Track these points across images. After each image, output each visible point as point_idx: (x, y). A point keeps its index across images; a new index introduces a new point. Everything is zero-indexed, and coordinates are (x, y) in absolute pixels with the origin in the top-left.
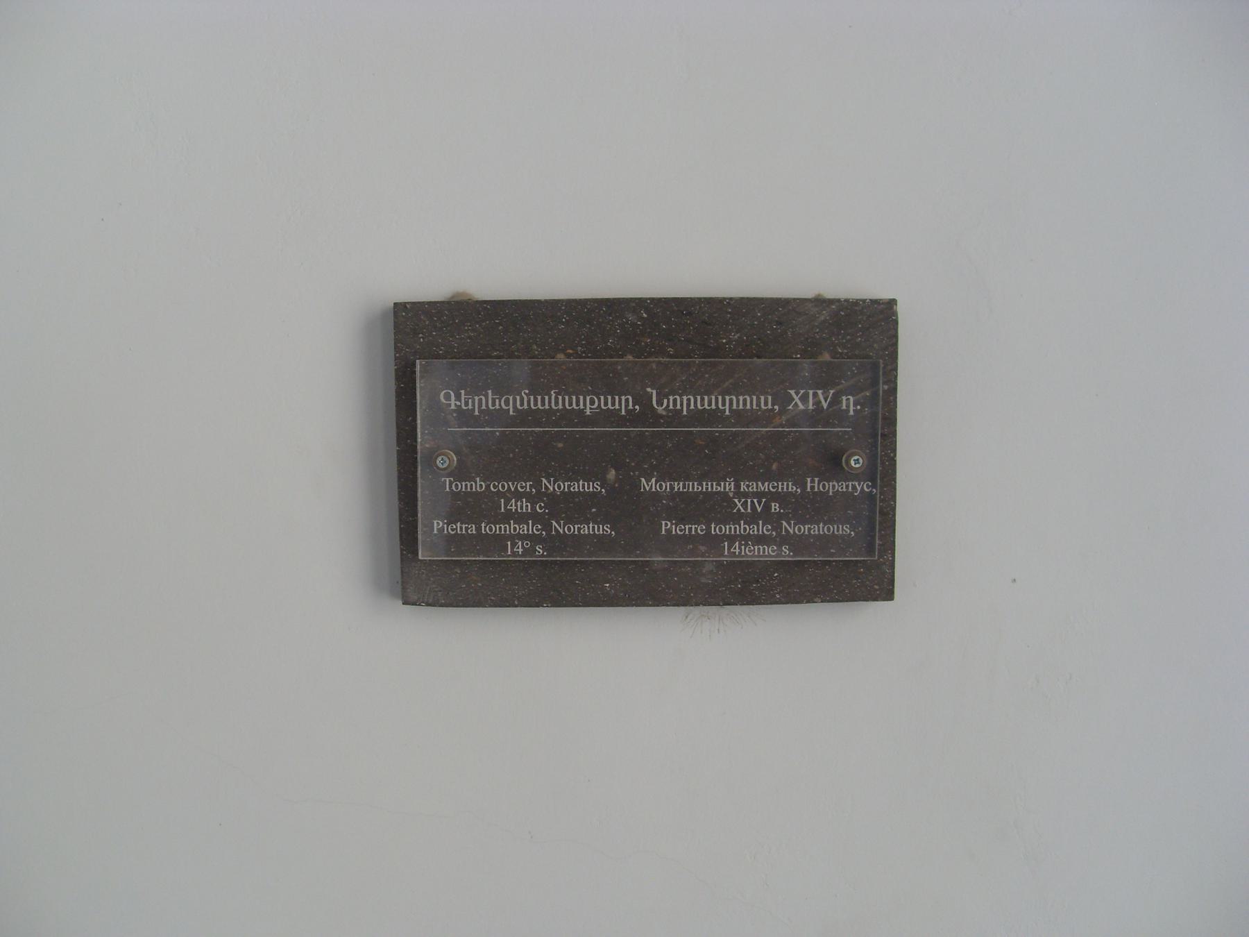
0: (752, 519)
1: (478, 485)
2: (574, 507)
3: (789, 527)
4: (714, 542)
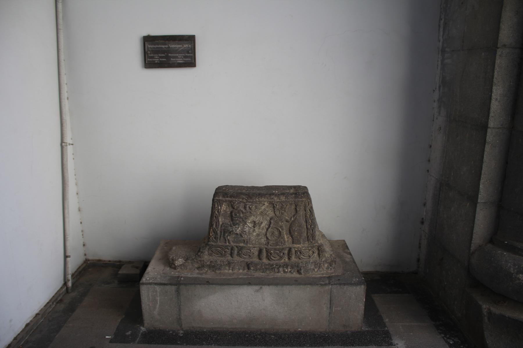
0: (180, 58)
1: (152, 55)
2: (161, 57)
3: (184, 59)
4: (177, 61)
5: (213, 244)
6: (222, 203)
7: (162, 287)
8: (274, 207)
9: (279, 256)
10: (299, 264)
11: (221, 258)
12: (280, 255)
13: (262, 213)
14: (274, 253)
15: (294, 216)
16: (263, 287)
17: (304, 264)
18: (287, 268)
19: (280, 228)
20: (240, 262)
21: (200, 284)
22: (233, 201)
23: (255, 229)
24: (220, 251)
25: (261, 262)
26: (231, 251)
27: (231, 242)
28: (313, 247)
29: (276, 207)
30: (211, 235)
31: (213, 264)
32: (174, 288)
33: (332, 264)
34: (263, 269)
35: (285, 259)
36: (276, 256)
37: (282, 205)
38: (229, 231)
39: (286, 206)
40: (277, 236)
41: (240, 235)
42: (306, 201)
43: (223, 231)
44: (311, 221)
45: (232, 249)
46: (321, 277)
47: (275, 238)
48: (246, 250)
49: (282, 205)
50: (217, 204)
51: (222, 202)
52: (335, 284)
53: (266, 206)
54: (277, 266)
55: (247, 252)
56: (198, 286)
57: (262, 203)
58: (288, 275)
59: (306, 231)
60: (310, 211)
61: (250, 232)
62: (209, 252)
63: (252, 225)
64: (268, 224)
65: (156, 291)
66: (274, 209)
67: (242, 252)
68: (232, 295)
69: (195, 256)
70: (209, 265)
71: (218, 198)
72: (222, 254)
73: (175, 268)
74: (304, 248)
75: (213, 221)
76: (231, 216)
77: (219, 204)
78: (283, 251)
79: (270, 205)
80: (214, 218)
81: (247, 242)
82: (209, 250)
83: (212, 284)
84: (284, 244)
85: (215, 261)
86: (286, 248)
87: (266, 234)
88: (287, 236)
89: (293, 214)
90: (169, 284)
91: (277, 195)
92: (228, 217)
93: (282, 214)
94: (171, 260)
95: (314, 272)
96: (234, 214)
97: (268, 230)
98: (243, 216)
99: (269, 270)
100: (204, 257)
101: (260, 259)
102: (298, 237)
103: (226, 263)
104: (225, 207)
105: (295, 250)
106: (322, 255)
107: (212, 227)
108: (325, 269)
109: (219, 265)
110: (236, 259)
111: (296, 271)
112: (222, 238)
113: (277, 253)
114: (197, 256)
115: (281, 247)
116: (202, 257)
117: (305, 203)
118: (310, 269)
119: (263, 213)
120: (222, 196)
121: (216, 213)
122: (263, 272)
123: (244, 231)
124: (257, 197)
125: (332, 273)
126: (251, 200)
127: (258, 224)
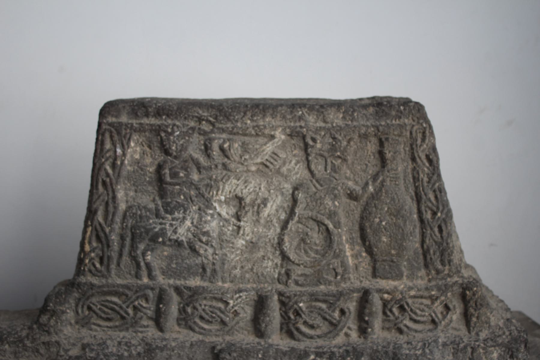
5: (95, 281)
6: (128, 136)
8: (306, 145)
11: (122, 334)
13: (267, 166)
14: (312, 312)
15: (375, 178)
17: (415, 348)
19: (328, 219)
20: (188, 344)
22: (167, 126)
23: (242, 223)
24: (117, 308)
25: (263, 343)
26: (157, 306)
27: (157, 273)
28: (444, 289)
29: (312, 147)
30: (87, 248)
31: (93, 355)
33: (518, 350)
35: (349, 332)
36: (318, 321)
37: (334, 138)
38: (151, 234)
39: (349, 142)
40: (319, 248)
41: (191, 248)
42: (413, 126)
43: (129, 234)
44: (436, 197)
45: (161, 298)
47: (313, 255)
48: (210, 303)
49: (334, 138)
50: (111, 137)
51: (128, 131)
53: (280, 143)
55: (214, 307)
57: (267, 132)
59: (417, 230)
60: (430, 161)
61: (225, 237)
62: (80, 311)
63: (232, 211)
64: (285, 205)
66: (307, 155)
67: (195, 308)
69: (30, 328)
71: (114, 120)
72: (123, 318)
75: (96, 200)
77: (116, 137)
78: (341, 304)
79: (293, 142)
81: (214, 271)
82: (81, 303)
84: (344, 279)
85: (99, 345)
86: (353, 291)
87: (281, 242)
88: (352, 250)
89: (371, 171)
92: (150, 183)
93: (335, 169)
96: (167, 171)
98: (201, 180)
100: (61, 331)
101: (259, 333)
102: (393, 252)
103: (140, 349)
104: (138, 149)
105: (382, 299)
106: (478, 318)
107: (92, 222)
110: (174, 335)
112: (126, 258)
113: (320, 308)
114: (35, 326)
115: (333, 288)
116: (52, 330)
117: (411, 133)
119: (267, 169)
120: (128, 113)
121: (105, 169)
123: (205, 230)
124: (249, 114)
126: (229, 125)
127: (253, 207)
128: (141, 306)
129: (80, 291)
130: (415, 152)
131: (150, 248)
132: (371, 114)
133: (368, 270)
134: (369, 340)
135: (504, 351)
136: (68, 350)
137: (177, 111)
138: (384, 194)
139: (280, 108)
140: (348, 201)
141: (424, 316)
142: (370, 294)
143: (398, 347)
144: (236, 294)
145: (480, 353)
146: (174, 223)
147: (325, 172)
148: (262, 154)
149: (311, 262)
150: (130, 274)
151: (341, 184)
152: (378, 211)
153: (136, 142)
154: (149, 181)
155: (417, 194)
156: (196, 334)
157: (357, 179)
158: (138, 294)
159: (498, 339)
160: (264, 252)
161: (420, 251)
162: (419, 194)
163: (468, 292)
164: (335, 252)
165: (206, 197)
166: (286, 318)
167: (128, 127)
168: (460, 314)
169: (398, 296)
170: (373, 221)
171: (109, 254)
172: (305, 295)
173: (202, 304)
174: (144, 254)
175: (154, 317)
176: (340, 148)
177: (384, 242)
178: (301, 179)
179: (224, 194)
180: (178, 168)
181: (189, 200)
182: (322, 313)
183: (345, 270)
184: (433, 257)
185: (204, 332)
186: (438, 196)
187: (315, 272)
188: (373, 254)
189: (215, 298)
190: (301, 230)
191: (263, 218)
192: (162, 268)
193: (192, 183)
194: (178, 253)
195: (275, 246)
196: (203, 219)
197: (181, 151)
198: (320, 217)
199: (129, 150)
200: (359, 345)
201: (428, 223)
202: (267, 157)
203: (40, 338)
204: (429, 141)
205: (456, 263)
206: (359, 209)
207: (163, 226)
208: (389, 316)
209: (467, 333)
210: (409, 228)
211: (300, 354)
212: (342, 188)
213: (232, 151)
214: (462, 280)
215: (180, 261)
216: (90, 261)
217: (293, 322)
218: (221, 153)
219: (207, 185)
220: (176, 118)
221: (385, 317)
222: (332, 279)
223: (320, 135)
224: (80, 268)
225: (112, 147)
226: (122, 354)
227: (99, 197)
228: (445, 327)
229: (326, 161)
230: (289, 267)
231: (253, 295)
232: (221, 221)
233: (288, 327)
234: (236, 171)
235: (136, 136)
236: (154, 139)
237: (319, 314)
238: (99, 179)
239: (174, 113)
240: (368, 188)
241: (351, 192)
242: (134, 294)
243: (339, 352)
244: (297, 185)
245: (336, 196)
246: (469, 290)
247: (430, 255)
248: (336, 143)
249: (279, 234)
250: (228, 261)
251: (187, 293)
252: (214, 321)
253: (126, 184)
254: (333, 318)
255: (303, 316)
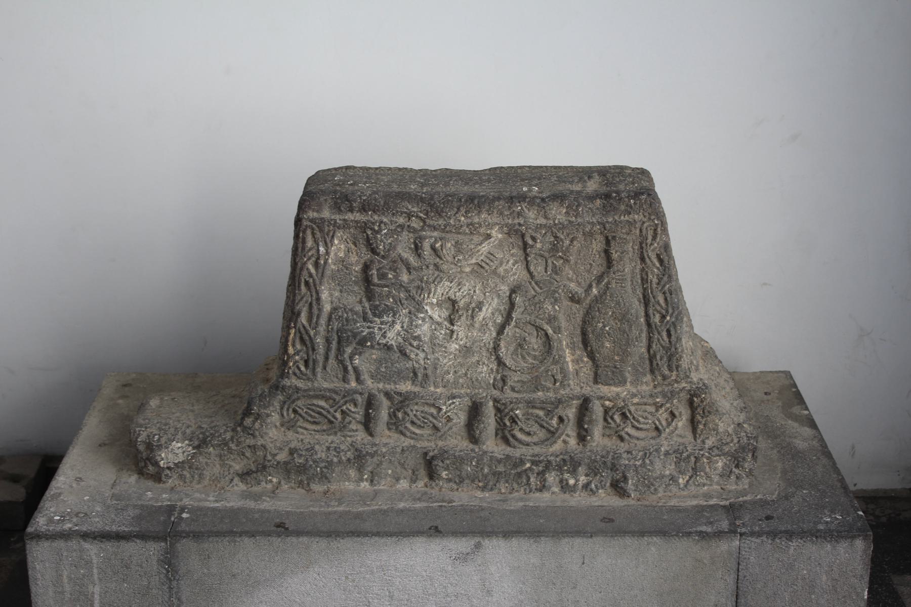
5: (300, 384)
6: (331, 234)
7: (109, 546)
8: (525, 246)
9: (544, 430)
10: (617, 457)
11: (330, 438)
12: (548, 424)
13: (482, 267)
14: (528, 419)
15: (599, 279)
16: (486, 542)
17: (635, 459)
18: (574, 472)
19: (547, 324)
20: (399, 450)
21: (252, 535)
22: (373, 224)
23: (455, 328)
24: (325, 413)
25: (477, 450)
26: (367, 410)
27: (365, 376)
29: (532, 247)
30: (291, 350)
32: (154, 549)
33: (744, 459)
34: (485, 476)
35: (568, 439)
36: (535, 428)
37: (556, 237)
39: (572, 241)
40: (537, 353)
41: (400, 351)
42: (644, 223)
43: (336, 338)
44: (666, 299)
45: (370, 403)
46: (700, 509)
47: (531, 361)
48: (421, 408)
49: (556, 237)
50: (313, 234)
52: (752, 534)
54: (537, 465)
56: (246, 540)
58: (579, 499)
59: (644, 335)
60: (661, 261)
62: (285, 414)
63: (445, 314)
64: (502, 308)
65: (89, 563)
66: (527, 255)
67: (405, 413)
68: (372, 573)
69: (234, 430)
70: (286, 463)
71: (315, 215)
72: (331, 422)
73: (158, 477)
74: (636, 400)
75: (299, 301)
76: (367, 281)
77: (318, 235)
78: (560, 411)
80: (303, 287)
82: (286, 406)
83: (299, 533)
84: (563, 385)
85: (307, 450)
86: (572, 399)
87: (496, 348)
90: (134, 536)
91: (538, 201)
92: (356, 283)
93: (556, 270)
94: (141, 448)
95: (674, 489)
96: (374, 272)
97: (503, 333)
99: (507, 482)
101: (474, 439)
102: (616, 358)
103: (349, 454)
104: (342, 246)
105: (603, 406)
106: (705, 425)
108: (716, 478)
109: (323, 465)
110: (385, 440)
111: (608, 484)
112: (332, 361)
114: (239, 429)
115: (551, 394)
116: (257, 433)
117: (641, 231)
118: (662, 476)
119: (482, 270)
120: (330, 207)
121: (308, 269)
122: (483, 489)
123: (416, 334)
124: (463, 210)
125: (744, 493)
126: (441, 222)
127: (467, 311)
128: (350, 410)
129: (284, 394)
130: (644, 251)
131: (358, 351)
132: (598, 209)
133: (589, 375)
134: (588, 447)
135: (730, 461)
136: (276, 455)
137: (384, 206)
138: (608, 297)
139: (497, 203)
140: (569, 303)
141: (647, 424)
142: (590, 401)
143: (618, 457)
144: (449, 401)
145: (704, 463)
146: (383, 326)
147: (545, 274)
148: (477, 254)
149: (528, 369)
150: (337, 377)
151: (562, 287)
152: (602, 315)
153: (340, 239)
154: (355, 280)
155: (644, 297)
156: (407, 439)
157: (580, 280)
158: (346, 399)
159: (724, 448)
160: (478, 357)
161: (646, 356)
162: (647, 297)
163: (695, 399)
164: (554, 358)
165: (416, 300)
166: (501, 424)
167: (331, 224)
168: (687, 420)
169: (620, 403)
170: (596, 326)
171: (315, 358)
172: (522, 403)
173: (414, 409)
174: (351, 358)
175: (363, 421)
176: (562, 248)
177: (607, 347)
178: (519, 280)
179: (436, 297)
180: (386, 269)
181: (399, 303)
182: (539, 420)
183: (565, 377)
184: (659, 363)
185: (415, 437)
186: (668, 299)
187: (532, 378)
188: (595, 359)
189: (427, 404)
190: (518, 335)
191: (477, 322)
192: (370, 371)
193: (401, 285)
194: (387, 356)
195: (490, 350)
196: (414, 323)
197: (389, 250)
198: (539, 322)
199: (333, 248)
200: (577, 454)
201: (656, 327)
202: (482, 258)
203: (245, 441)
204: (661, 239)
205: (685, 367)
206: (581, 312)
207: (371, 330)
208: (610, 424)
209: (693, 440)
210: (635, 332)
211: (516, 462)
212: (563, 291)
213: (444, 251)
214: (691, 387)
215: (390, 365)
216: (294, 364)
217: (509, 429)
218: (432, 252)
219: (418, 287)
220: (383, 214)
221: (606, 424)
222: (551, 386)
223: (540, 233)
224: (284, 370)
225: (314, 245)
226: (332, 461)
227: (302, 298)
228: (669, 434)
229: (546, 262)
230: (505, 373)
231: (467, 401)
232: (432, 324)
233: (503, 433)
234: (449, 272)
235: (339, 233)
236: (360, 236)
237: (536, 422)
238: (301, 280)
239: (381, 209)
240: (592, 290)
241: (573, 296)
242: (342, 399)
243: (556, 461)
244: (515, 287)
245: (556, 300)
246: (697, 397)
247: (656, 361)
248: (558, 243)
249: (495, 338)
250: (441, 365)
251: (397, 398)
252: (426, 427)
253: (330, 284)
254: (550, 426)
255: (519, 423)
